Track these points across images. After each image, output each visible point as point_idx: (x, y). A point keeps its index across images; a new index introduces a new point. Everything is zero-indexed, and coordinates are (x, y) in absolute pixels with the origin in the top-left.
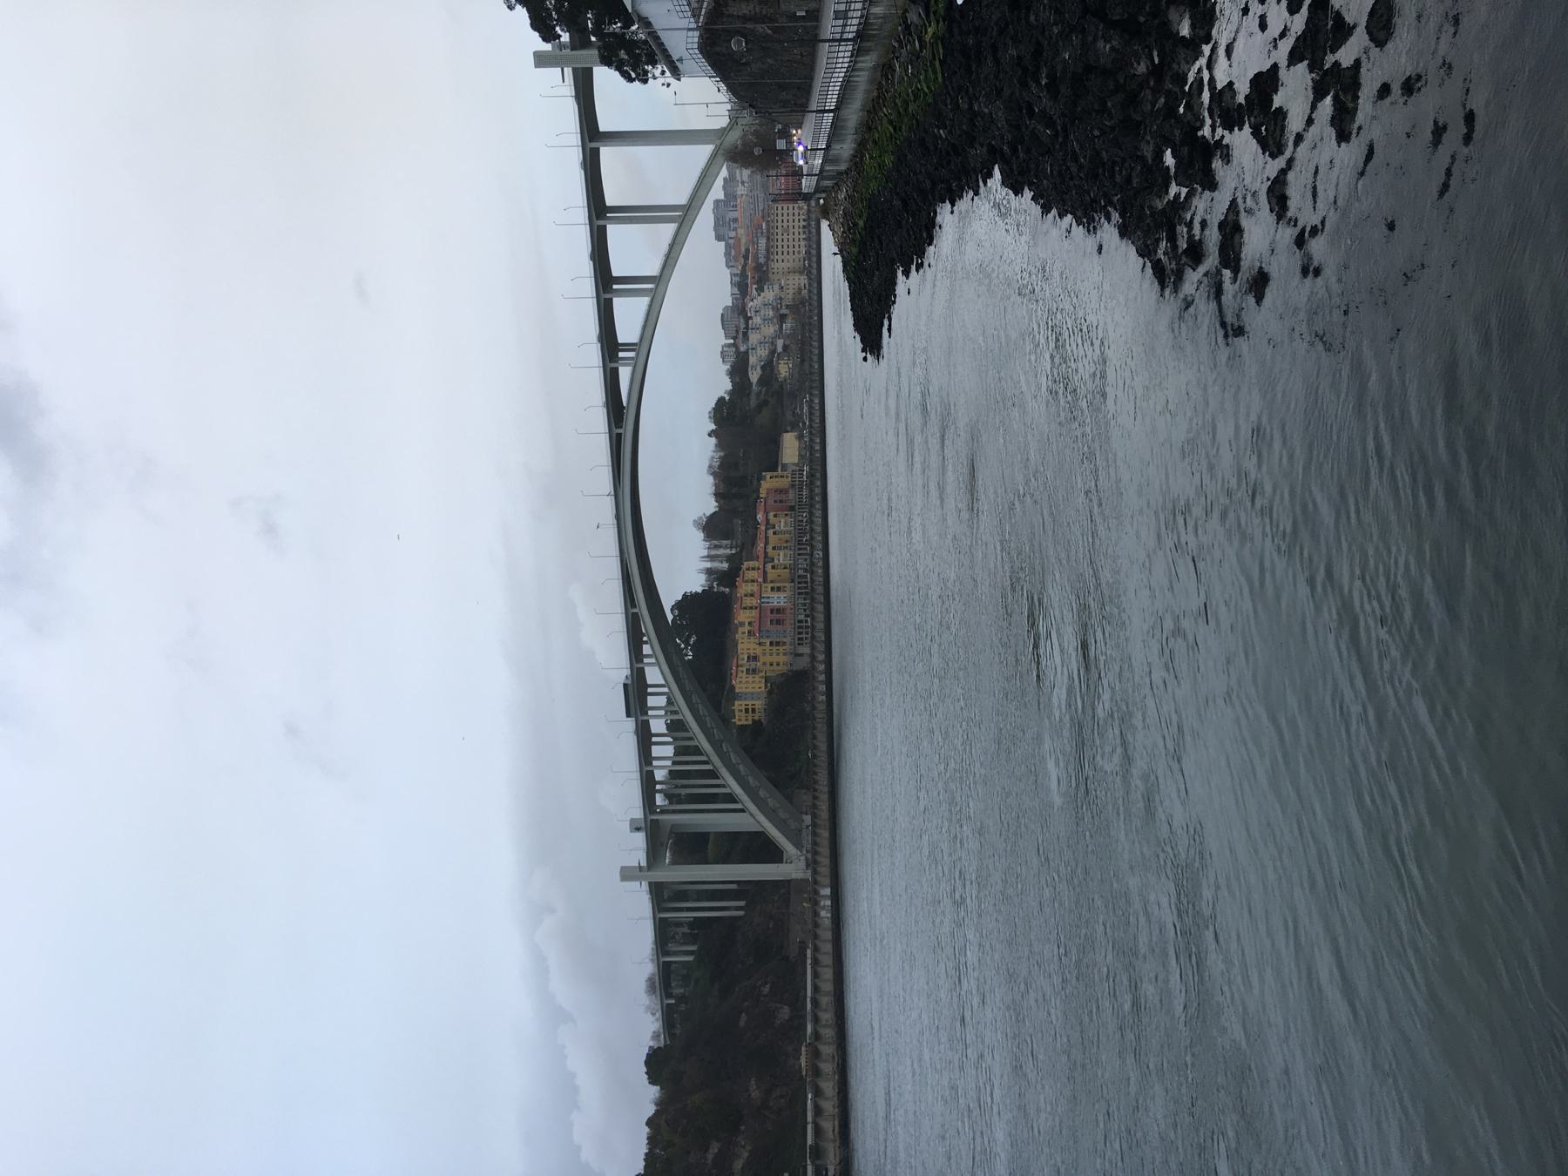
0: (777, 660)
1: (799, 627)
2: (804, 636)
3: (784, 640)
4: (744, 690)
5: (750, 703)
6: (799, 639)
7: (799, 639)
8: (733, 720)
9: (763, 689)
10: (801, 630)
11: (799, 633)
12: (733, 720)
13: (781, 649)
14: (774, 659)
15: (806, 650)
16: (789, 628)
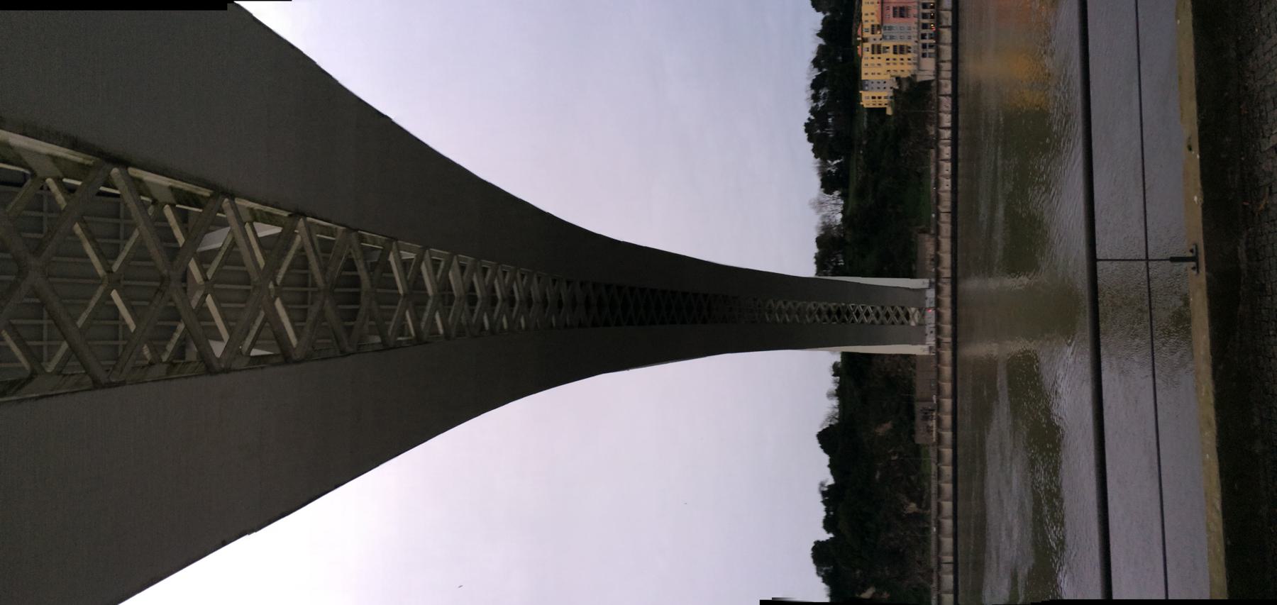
0: (905, 68)
1: (925, 26)
2: (927, 41)
3: (909, 45)
4: (869, 77)
5: (876, 94)
6: (924, 46)
7: (924, 46)
8: (861, 103)
9: (888, 77)
10: (924, 31)
11: (923, 37)
12: (861, 103)
13: (905, 57)
14: (899, 67)
15: (929, 64)
16: (911, 23)
